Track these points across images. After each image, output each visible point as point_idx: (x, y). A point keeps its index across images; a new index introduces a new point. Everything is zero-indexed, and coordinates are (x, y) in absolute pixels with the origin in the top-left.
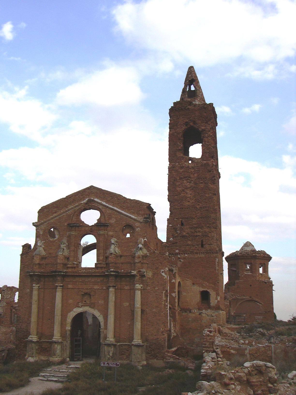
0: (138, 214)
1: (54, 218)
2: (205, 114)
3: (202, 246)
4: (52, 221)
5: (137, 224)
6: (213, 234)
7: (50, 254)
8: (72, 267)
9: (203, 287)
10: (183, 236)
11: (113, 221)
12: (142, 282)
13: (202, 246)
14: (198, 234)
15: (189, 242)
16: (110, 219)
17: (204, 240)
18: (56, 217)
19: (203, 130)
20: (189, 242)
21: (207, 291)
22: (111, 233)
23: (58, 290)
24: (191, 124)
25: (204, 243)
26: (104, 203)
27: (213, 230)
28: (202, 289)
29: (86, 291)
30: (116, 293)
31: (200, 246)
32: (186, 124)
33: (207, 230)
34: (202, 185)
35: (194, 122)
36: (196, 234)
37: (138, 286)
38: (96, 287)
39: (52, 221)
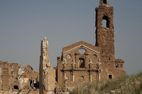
0: (98, 51)
1: (69, 51)
2: (111, 11)
3: (109, 60)
4: (69, 52)
5: (98, 54)
6: (113, 56)
7: (69, 63)
8: (77, 68)
9: (110, 73)
10: (103, 56)
11: (90, 53)
12: (100, 73)
13: (109, 60)
14: (108, 55)
15: (105, 58)
16: (89, 52)
17: (110, 58)
18: (70, 51)
19: (110, 18)
20: (105, 58)
21: (111, 75)
22: (89, 57)
23: (73, 75)
24: (106, 15)
25: (110, 59)
26: (87, 47)
27: (113, 54)
28: (109, 74)
29: (82, 75)
30: (92, 76)
31: (109, 60)
32: (104, 14)
33: (111, 54)
34: (109, 38)
35: (107, 14)
36: (107, 55)
37: (99, 74)
38: (85, 74)
39: (69, 52)
